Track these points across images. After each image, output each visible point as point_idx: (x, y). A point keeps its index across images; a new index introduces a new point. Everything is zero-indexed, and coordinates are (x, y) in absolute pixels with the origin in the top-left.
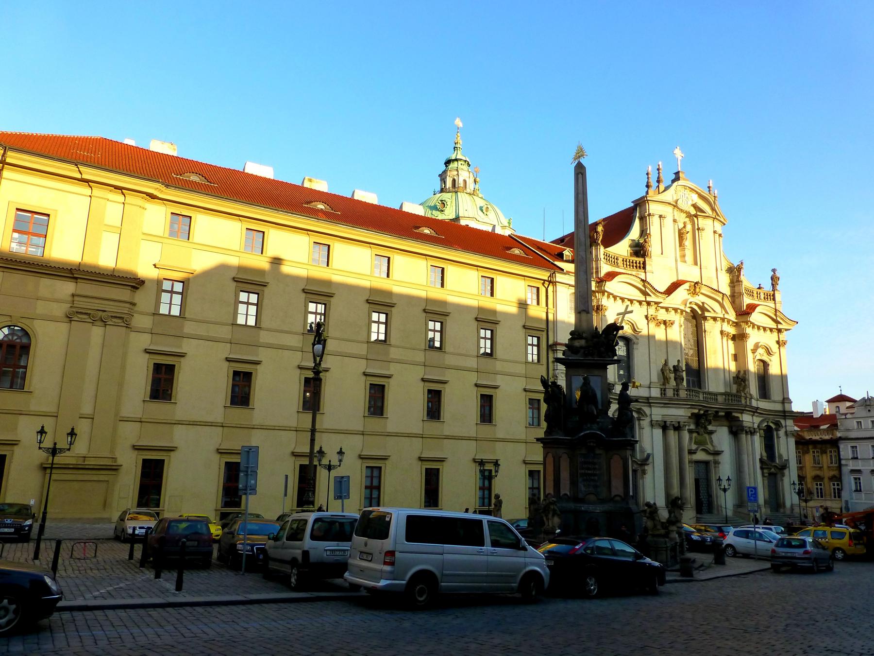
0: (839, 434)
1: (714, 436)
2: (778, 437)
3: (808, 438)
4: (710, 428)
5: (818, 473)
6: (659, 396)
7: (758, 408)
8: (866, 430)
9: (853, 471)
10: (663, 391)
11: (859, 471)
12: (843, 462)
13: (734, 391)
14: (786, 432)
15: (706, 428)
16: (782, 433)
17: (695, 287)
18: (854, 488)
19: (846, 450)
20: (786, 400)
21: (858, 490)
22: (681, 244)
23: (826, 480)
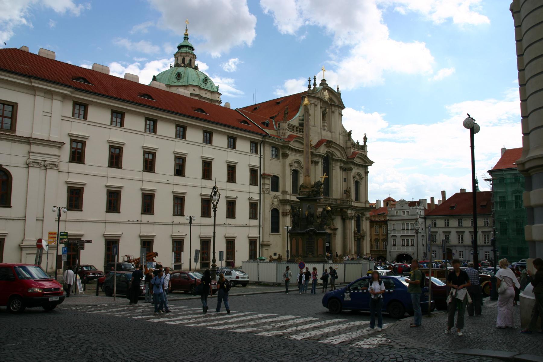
0: (388, 218)
1: (334, 222)
2: (363, 221)
3: (373, 219)
4: (333, 217)
5: (377, 237)
7: (355, 206)
8: (401, 216)
9: (393, 236)
11: (395, 236)
12: (389, 232)
13: (344, 198)
15: (331, 217)
16: (364, 219)
17: (329, 143)
19: (390, 226)
20: (367, 202)
21: (394, 245)
22: (323, 119)
23: (380, 241)
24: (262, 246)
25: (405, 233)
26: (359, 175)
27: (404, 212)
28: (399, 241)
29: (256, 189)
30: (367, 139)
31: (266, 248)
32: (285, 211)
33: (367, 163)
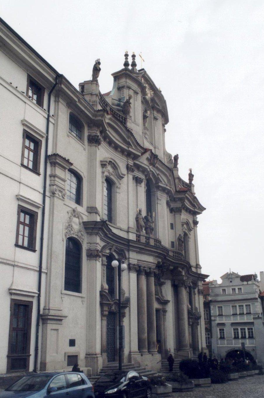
0: (210, 299)
2: (195, 294)
6: (135, 240)
8: (229, 295)
9: (219, 324)
10: (138, 236)
11: (223, 324)
12: (213, 318)
14: (199, 290)
18: (219, 337)
21: (222, 338)
24: (43, 319)
25: (239, 319)
26: (187, 224)
27: (234, 290)
28: (229, 331)
29: (36, 181)
30: (193, 176)
31: (55, 327)
32: (93, 247)
33: (196, 208)
